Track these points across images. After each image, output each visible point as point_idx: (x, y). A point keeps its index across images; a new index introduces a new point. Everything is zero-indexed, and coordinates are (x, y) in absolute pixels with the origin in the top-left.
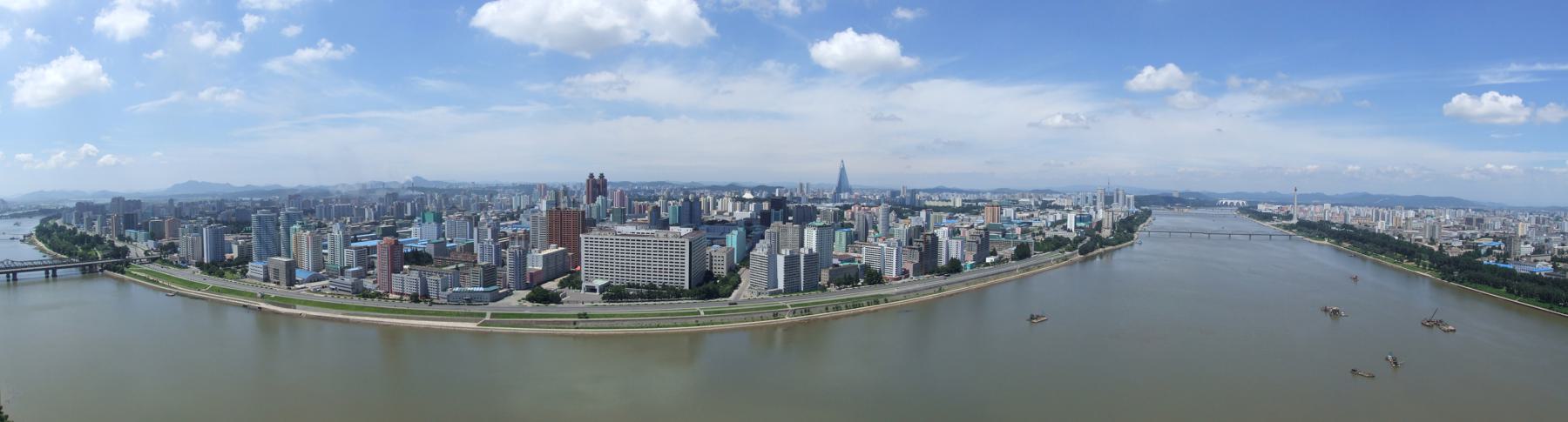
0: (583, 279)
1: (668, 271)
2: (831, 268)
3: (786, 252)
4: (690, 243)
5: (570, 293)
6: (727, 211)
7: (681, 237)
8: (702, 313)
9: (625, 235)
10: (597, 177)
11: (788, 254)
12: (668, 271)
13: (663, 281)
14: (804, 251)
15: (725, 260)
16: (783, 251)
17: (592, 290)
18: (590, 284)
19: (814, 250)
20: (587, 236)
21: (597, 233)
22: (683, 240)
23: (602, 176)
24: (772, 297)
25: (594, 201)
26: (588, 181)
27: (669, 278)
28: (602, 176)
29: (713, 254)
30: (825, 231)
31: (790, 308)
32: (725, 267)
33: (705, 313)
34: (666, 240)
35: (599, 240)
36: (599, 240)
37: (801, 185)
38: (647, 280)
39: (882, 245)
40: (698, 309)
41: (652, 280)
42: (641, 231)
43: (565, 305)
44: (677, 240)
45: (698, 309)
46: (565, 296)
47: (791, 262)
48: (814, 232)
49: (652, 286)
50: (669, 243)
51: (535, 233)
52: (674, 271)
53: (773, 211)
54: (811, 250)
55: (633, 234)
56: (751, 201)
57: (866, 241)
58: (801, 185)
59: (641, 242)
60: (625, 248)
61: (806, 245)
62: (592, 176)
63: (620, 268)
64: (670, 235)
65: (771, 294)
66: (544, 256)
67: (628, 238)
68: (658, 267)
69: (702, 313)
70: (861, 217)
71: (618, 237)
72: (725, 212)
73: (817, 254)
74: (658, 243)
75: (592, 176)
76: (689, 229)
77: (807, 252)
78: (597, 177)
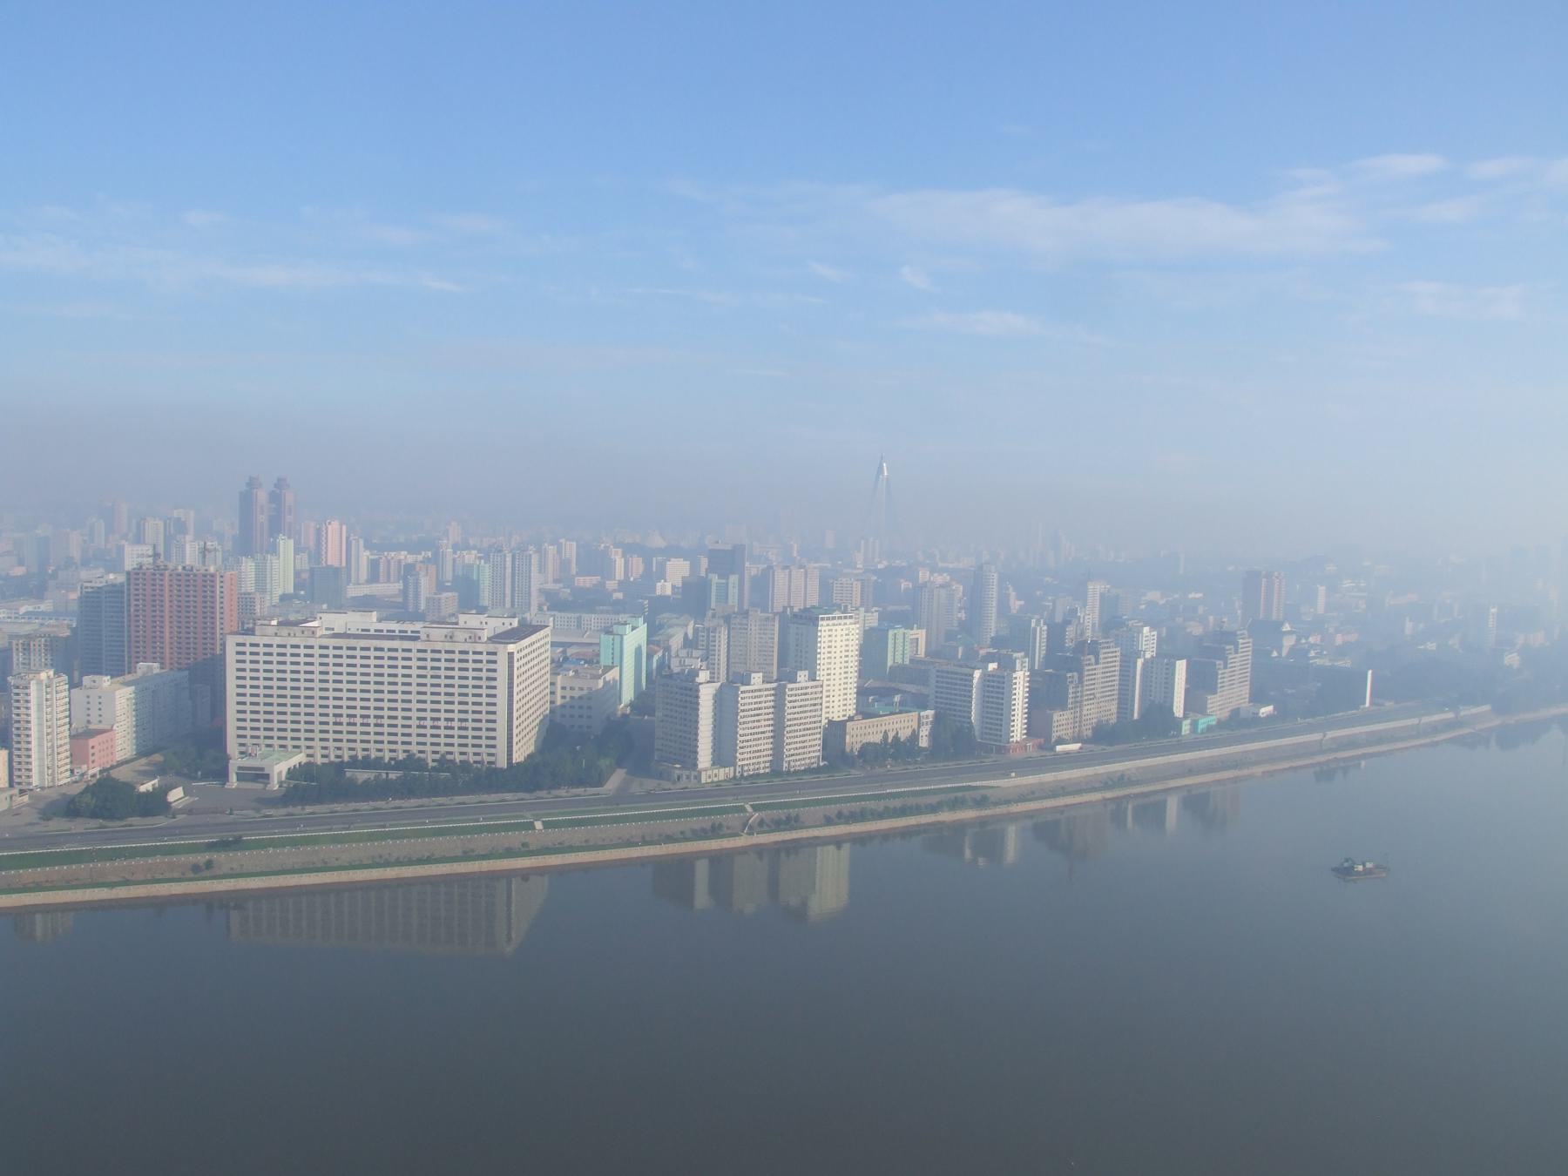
0: (232, 747)
1: (456, 724)
8: (539, 825)
13: (443, 749)
18: (247, 762)
27: (456, 741)
28: (281, 483)
33: (546, 825)
34: (449, 646)
35: (275, 650)
36: (275, 650)
38: (400, 747)
41: (414, 748)
42: (385, 626)
44: (479, 648)
49: (411, 763)
50: (457, 656)
53: (715, 578)
55: (365, 635)
59: (386, 654)
60: (344, 669)
64: (460, 636)
67: (352, 643)
68: (429, 715)
69: (539, 825)
71: (325, 642)
74: (429, 655)
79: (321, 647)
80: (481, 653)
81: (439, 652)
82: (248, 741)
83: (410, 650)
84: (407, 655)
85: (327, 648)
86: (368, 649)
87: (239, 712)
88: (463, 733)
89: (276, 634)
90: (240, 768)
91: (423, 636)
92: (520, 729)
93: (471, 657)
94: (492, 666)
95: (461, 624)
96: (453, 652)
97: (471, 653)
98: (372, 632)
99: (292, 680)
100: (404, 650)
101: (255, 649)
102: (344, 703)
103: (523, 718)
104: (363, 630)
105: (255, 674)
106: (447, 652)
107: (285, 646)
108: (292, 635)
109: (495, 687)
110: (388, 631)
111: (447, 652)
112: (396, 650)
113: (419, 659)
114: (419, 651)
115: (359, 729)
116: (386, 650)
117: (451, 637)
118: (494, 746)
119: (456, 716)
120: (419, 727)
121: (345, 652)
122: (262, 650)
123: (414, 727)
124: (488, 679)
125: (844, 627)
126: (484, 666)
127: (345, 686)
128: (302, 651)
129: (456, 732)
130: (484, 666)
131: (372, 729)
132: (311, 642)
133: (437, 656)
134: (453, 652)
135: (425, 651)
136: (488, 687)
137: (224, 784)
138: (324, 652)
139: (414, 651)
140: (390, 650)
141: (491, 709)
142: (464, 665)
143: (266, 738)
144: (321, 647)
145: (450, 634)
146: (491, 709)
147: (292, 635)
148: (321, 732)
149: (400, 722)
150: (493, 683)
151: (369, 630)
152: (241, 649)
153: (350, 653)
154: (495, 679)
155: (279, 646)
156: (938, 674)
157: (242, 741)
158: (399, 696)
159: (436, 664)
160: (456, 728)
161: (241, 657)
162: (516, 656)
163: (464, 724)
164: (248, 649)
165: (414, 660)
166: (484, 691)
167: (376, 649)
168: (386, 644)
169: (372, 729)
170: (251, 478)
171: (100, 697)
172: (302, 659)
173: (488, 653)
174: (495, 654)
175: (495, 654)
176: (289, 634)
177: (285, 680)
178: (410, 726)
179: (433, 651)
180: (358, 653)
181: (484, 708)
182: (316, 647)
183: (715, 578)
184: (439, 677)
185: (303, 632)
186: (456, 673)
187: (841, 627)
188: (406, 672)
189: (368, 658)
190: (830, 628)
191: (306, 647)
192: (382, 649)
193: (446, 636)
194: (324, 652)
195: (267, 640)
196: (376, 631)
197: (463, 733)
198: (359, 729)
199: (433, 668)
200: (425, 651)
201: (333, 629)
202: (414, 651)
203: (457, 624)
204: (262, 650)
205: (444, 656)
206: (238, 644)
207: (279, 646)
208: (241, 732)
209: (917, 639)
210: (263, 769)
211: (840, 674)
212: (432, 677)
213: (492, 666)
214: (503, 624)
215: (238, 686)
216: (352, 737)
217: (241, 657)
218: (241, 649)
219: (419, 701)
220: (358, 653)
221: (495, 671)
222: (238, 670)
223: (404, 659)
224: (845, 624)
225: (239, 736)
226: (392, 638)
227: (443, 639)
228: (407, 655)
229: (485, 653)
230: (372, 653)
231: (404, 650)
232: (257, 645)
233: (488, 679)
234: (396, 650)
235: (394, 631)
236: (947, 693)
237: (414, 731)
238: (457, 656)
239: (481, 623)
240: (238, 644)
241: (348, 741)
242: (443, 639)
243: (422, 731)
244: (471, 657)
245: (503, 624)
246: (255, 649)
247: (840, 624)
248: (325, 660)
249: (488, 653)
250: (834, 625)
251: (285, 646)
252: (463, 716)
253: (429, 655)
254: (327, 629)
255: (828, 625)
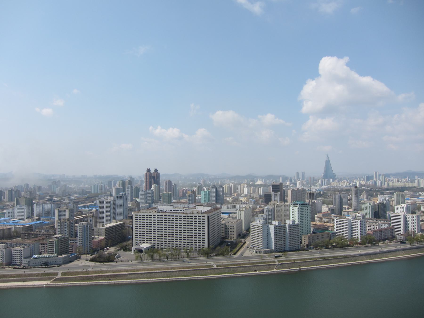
1: (194, 237)
2: (309, 234)
3: (275, 223)
4: (208, 217)
5: (124, 255)
6: (243, 193)
7: (202, 213)
9: (166, 212)
10: (152, 171)
11: (277, 224)
12: (194, 237)
14: (289, 222)
15: (235, 229)
16: (274, 222)
17: (140, 251)
18: (137, 247)
19: (297, 221)
20: (136, 213)
21: (145, 211)
22: (203, 215)
23: (156, 170)
24: (265, 255)
25: (150, 187)
26: (146, 173)
27: (194, 241)
28: (156, 170)
29: (227, 224)
30: (305, 208)
31: (277, 263)
32: (235, 233)
33: (217, 266)
34: (191, 215)
35: (145, 216)
36: (145, 216)
37: (298, 174)
39: (349, 218)
40: (212, 263)
43: (119, 263)
44: (200, 215)
45: (212, 263)
46: (119, 257)
47: (279, 230)
48: (297, 209)
50: (194, 218)
51: (102, 212)
52: (198, 237)
54: (293, 222)
55: (171, 212)
56: (260, 186)
57: (341, 214)
58: (298, 174)
60: (163, 222)
61: (291, 218)
62: (149, 170)
63: (160, 235)
64: (195, 212)
65: (266, 252)
66: (106, 229)
70: (337, 197)
72: (241, 194)
73: (298, 225)
74: (186, 217)
75: (149, 170)
76: (209, 207)
77: (291, 223)
78: (152, 171)
79: (157, 216)
80: (200, 217)
81: (189, 216)
82: (138, 241)
83: (181, 216)
84: (180, 217)
85: (159, 216)
86: (170, 216)
87: (136, 233)
88: (196, 239)
89: (146, 212)
90: (135, 249)
91: (185, 212)
92: (212, 238)
93: (197, 218)
94: (203, 220)
95: (197, 209)
96: (193, 216)
97: (197, 217)
98: (173, 211)
99: (150, 225)
100: (179, 216)
101: (140, 216)
102: (171, 231)
103: (213, 235)
104: (170, 210)
105: (151, 223)
106: (191, 216)
107: (148, 215)
108: (150, 212)
109: (204, 226)
110: (177, 211)
111: (191, 216)
112: (177, 216)
113: (183, 219)
114: (183, 216)
115: (167, 238)
116: (175, 216)
117: (192, 212)
118: (204, 243)
119: (194, 234)
120: (183, 237)
121: (163, 217)
122: (142, 216)
123: (182, 237)
124: (202, 224)
125: (306, 207)
126: (201, 220)
127: (164, 226)
128: (152, 217)
129: (194, 239)
130: (201, 220)
131: (171, 238)
132: (155, 214)
133: (188, 218)
134: (193, 216)
135: (185, 216)
136: (202, 226)
137: (131, 253)
138: (158, 217)
139: (182, 216)
140: (176, 216)
141: (203, 232)
142: (196, 220)
143: (143, 240)
144: (157, 216)
145: (192, 212)
146: (203, 232)
147: (150, 212)
148: (157, 239)
149: (178, 236)
150: (203, 225)
151: (172, 211)
152: (136, 216)
153: (165, 217)
154: (204, 224)
155: (146, 215)
156: (337, 220)
157: (137, 241)
158: (178, 229)
159: (188, 220)
160: (194, 238)
161: (136, 218)
162: (210, 218)
163: (196, 237)
164: (138, 216)
165: (182, 219)
166: (201, 227)
167: (172, 216)
168: (175, 214)
169: (171, 238)
170: (148, 169)
171: (98, 229)
172: (152, 219)
173: (202, 217)
174: (204, 217)
175: (204, 217)
176: (149, 212)
177: (141, 224)
178: (181, 237)
179: (187, 216)
180: (167, 217)
181: (201, 232)
182: (156, 216)
183: (273, 193)
184: (189, 223)
185: (153, 212)
186: (194, 222)
187: (305, 207)
188: (180, 222)
189: (161, 218)
190: (307, 207)
191: (153, 216)
192: (173, 216)
193: (191, 212)
194: (158, 217)
195: (143, 214)
196: (174, 211)
197: (196, 239)
198: (167, 238)
199: (187, 221)
200: (185, 216)
201: (162, 210)
202: (182, 216)
203: (195, 208)
204: (142, 216)
205: (190, 218)
206: (136, 215)
207: (146, 215)
208: (137, 239)
209: (334, 209)
210: (141, 249)
211: (306, 221)
212: (187, 223)
213: (203, 220)
214: (208, 208)
215: (136, 226)
216: (166, 240)
217: (136, 218)
218: (136, 216)
219: (183, 230)
220: (167, 217)
221: (204, 221)
222: (136, 222)
223: (179, 218)
224: (307, 206)
225: (136, 240)
226: (176, 213)
227: (190, 213)
228: (180, 217)
229: (201, 217)
230: (171, 217)
231: (179, 216)
232: (141, 215)
233: (202, 224)
234: (177, 216)
235: (182, 211)
236: (340, 226)
237: (182, 238)
238: (194, 218)
239: (202, 208)
240: (136, 215)
241: (161, 241)
242: (190, 213)
243: (184, 239)
244: (197, 218)
245: (208, 208)
246: (140, 216)
247: (305, 206)
248: (158, 219)
249: (202, 217)
250: (303, 207)
251: (148, 215)
252: (196, 234)
253: (186, 217)
254: (161, 210)
255: (301, 207)
